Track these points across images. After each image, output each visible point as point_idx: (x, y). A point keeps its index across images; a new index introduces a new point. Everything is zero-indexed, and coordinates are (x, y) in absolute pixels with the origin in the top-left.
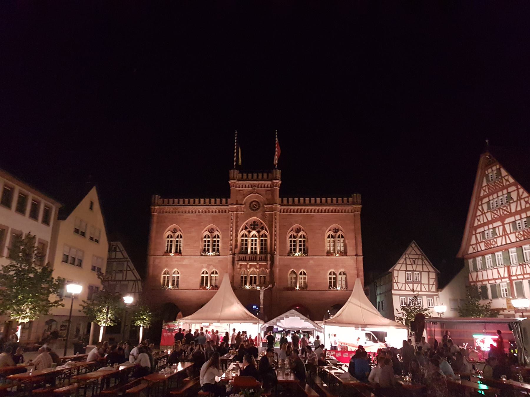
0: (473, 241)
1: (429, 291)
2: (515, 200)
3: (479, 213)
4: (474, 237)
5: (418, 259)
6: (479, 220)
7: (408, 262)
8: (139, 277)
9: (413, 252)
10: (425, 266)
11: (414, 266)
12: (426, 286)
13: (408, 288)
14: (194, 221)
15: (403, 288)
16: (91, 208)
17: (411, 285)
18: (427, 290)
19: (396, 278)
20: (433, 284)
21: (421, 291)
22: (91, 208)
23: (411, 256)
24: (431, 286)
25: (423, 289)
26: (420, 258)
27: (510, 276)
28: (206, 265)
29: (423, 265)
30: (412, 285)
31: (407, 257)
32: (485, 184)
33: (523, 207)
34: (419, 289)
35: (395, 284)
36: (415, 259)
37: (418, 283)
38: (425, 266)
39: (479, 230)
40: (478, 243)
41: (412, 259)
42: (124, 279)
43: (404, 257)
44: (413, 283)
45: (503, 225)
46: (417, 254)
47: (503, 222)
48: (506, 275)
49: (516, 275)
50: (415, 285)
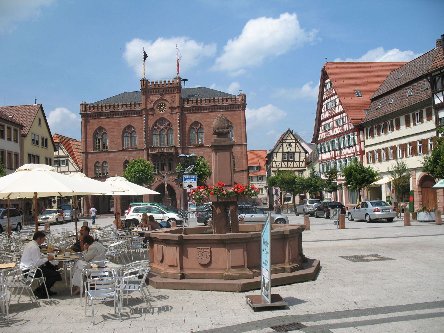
0: (320, 132)
1: (300, 167)
2: (338, 104)
3: (323, 111)
4: (321, 127)
5: (292, 142)
6: (323, 117)
7: (285, 145)
8: (78, 169)
9: (290, 138)
10: (297, 148)
11: (289, 149)
12: (298, 163)
13: (283, 165)
14: (115, 122)
15: (280, 166)
16: (40, 124)
17: (286, 163)
18: (299, 166)
19: (275, 158)
20: (303, 162)
21: (294, 167)
22: (40, 124)
23: (287, 141)
24: (301, 163)
25: (295, 166)
26: (294, 141)
27: (335, 157)
28: (127, 156)
29: (295, 147)
30: (287, 162)
31: (284, 141)
32: (325, 90)
33: (341, 110)
34: (292, 165)
35: (274, 163)
36: (290, 143)
37: (292, 161)
38: (297, 148)
39: (324, 123)
40: (322, 133)
41: (288, 143)
42: (67, 170)
43: (282, 142)
44: (288, 161)
45: (333, 121)
46: (292, 139)
47: (333, 119)
48: (333, 156)
49: (338, 156)
50: (290, 163)
